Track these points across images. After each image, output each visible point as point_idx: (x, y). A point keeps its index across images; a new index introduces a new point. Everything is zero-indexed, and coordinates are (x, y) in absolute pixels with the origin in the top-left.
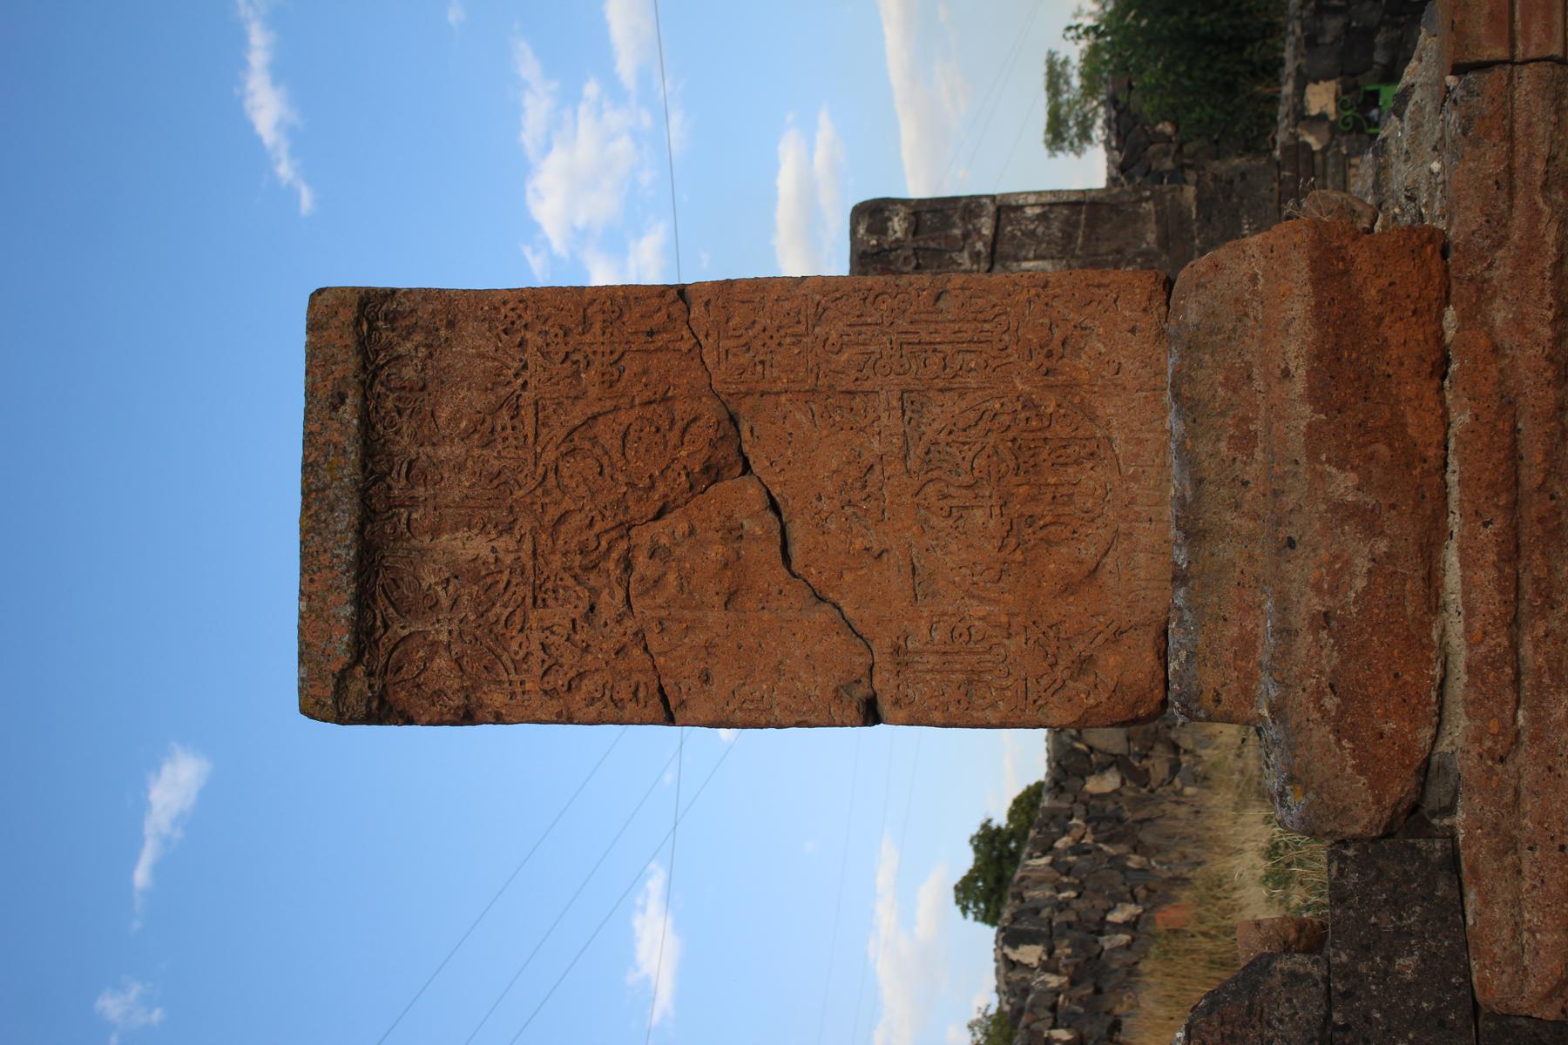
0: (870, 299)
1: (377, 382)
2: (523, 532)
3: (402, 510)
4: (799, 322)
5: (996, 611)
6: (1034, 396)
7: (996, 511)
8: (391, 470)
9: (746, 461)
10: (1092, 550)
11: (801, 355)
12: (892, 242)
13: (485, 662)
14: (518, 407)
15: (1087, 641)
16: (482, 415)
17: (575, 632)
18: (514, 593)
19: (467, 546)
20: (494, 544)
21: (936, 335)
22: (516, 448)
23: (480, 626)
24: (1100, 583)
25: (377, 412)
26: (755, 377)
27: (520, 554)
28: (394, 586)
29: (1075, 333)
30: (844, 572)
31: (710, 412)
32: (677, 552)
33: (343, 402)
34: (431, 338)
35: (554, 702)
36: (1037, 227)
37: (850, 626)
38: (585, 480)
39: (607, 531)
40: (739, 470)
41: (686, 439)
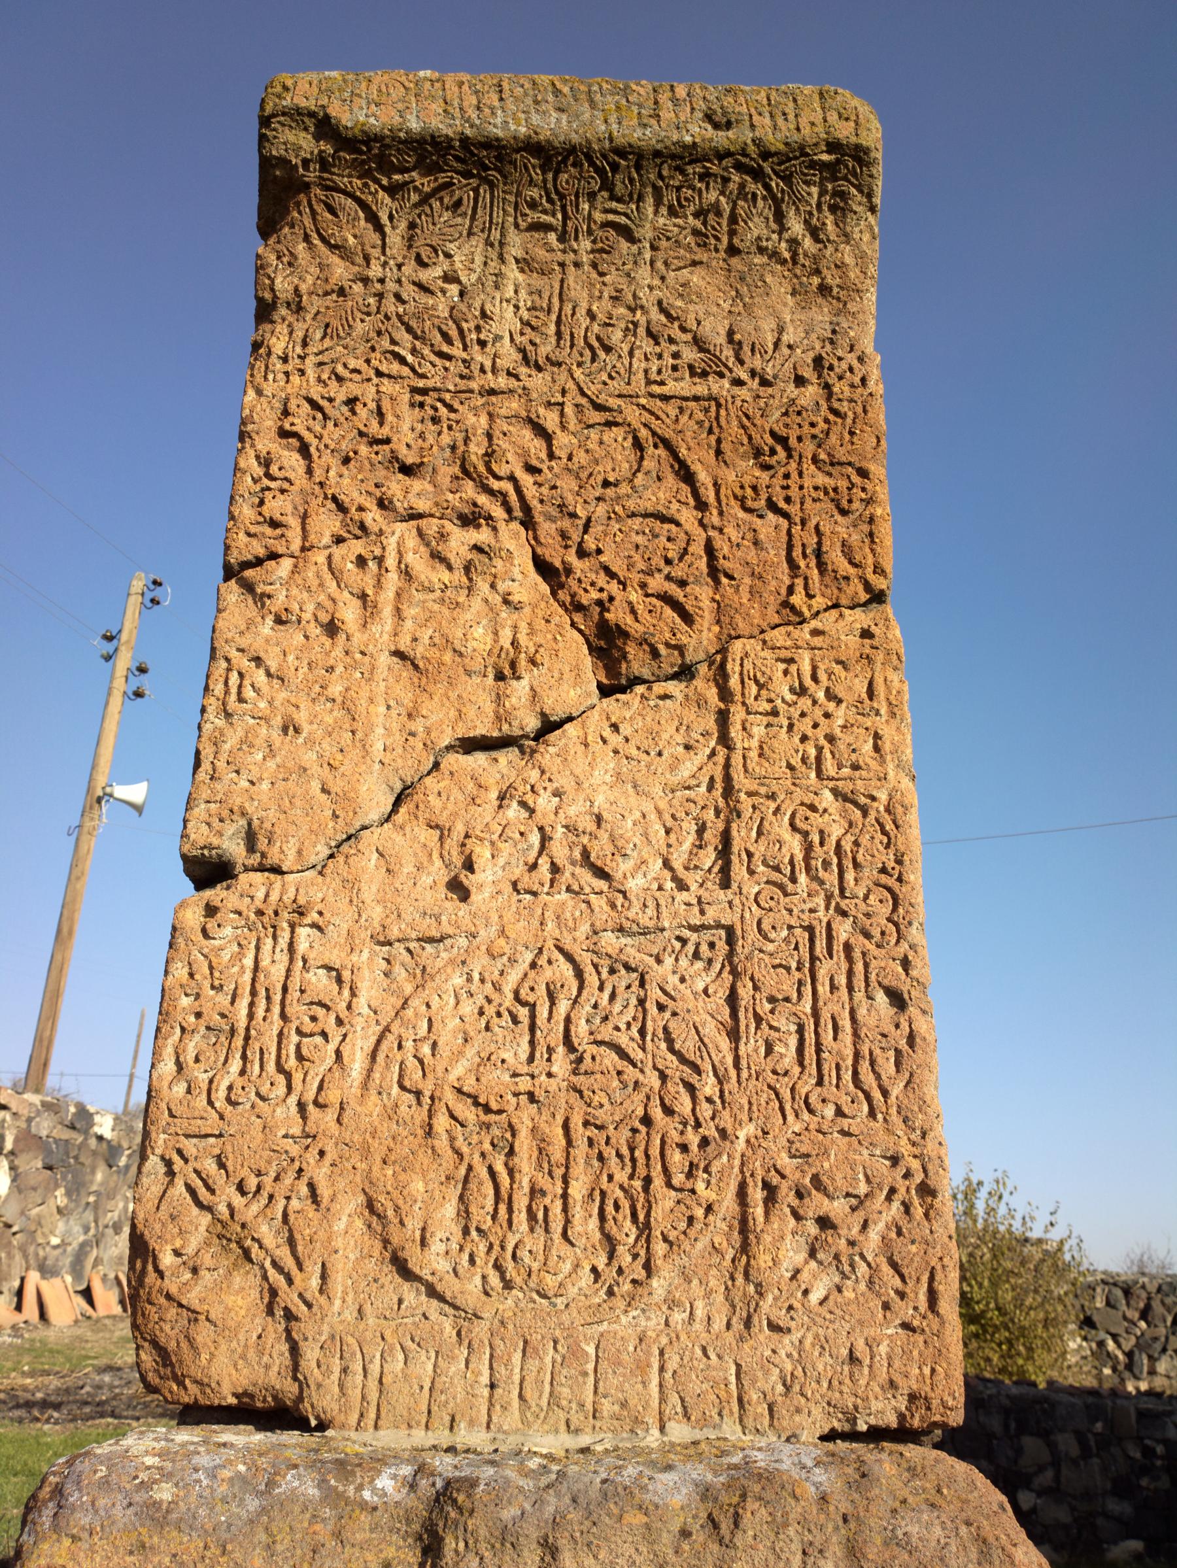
0: (884, 879)
3: (559, 216)
6: (725, 1158)
7: (524, 1084)
8: (619, 200)
21: (828, 988)
26: (750, 701)
29: (843, 1241)
33: (716, 126)
41: (654, 600)
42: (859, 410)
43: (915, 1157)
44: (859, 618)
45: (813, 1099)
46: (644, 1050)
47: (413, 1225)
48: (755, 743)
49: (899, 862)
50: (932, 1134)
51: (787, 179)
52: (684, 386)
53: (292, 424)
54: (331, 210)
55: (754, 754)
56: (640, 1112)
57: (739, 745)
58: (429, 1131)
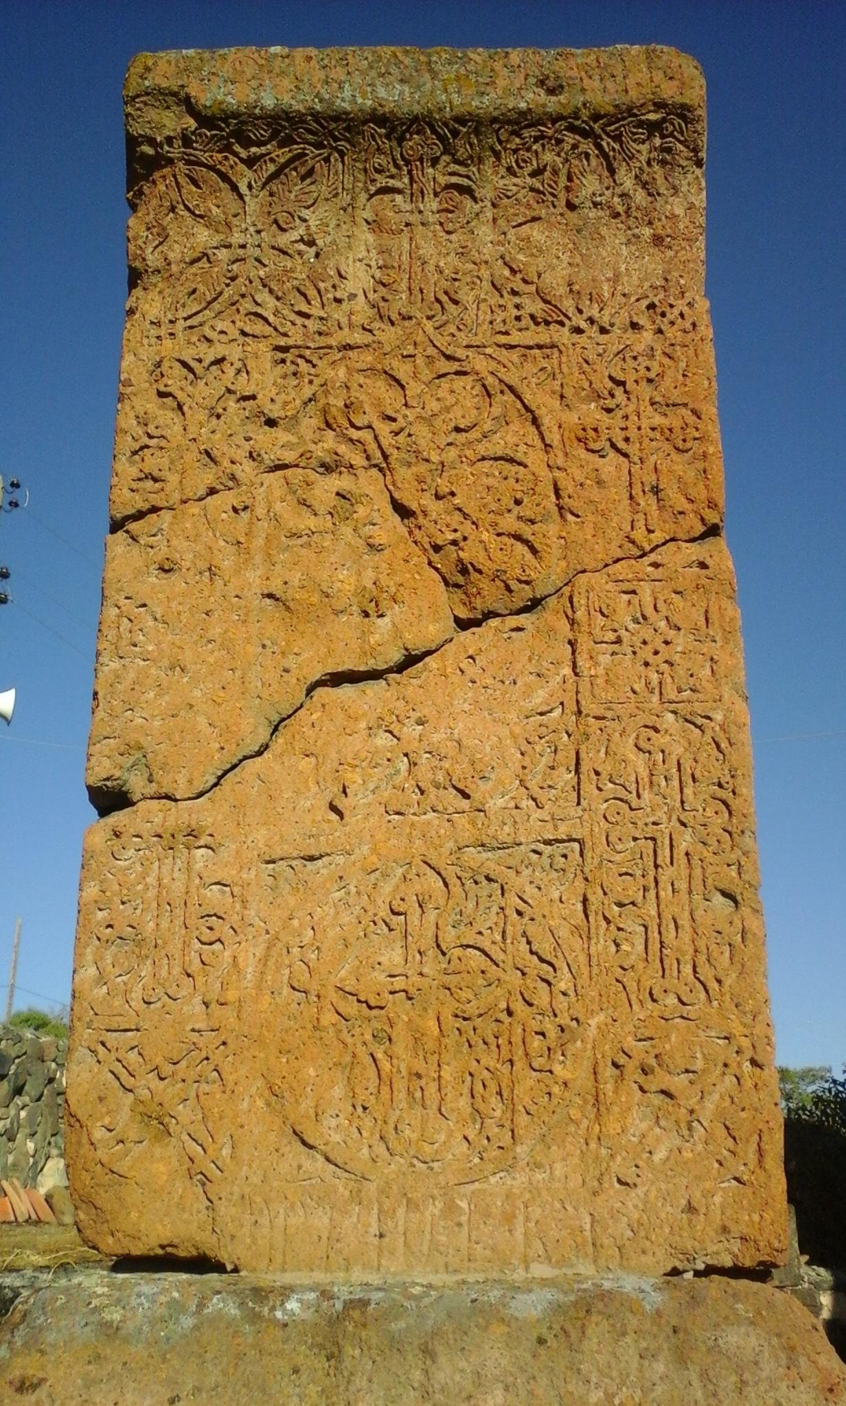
1: (577, 137)
2: (375, 332)
3: (406, 180)
4: (680, 691)
5: (245, 983)
6: (579, 1043)
7: (399, 983)
9: (478, 623)
10: (336, 1138)
11: (631, 694)
13: (201, 288)
14: (547, 323)
15: (191, 1129)
16: (536, 280)
17: (238, 401)
18: (294, 324)
19: (358, 264)
20: (361, 298)
22: (491, 323)
23: (251, 282)
24: (285, 1150)
25: (536, 140)
26: (597, 631)
27: (346, 330)
28: (303, 170)
29: (683, 1110)
30: (313, 760)
31: (548, 575)
32: (346, 530)
33: (551, 92)
34: (639, 216)
35: (145, 376)
37: (234, 767)
38: (447, 410)
39: (376, 437)
40: (464, 614)
41: (505, 539)
42: (691, 352)
44: (695, 551)
47: (306, 1105)
48: (601, 671)
50: (760, 1017)
51: (617, 138)
53: (166, 386)
54: (195, 183)
55: (600, 681)
56: (503, 1005)
57: (585, 673)
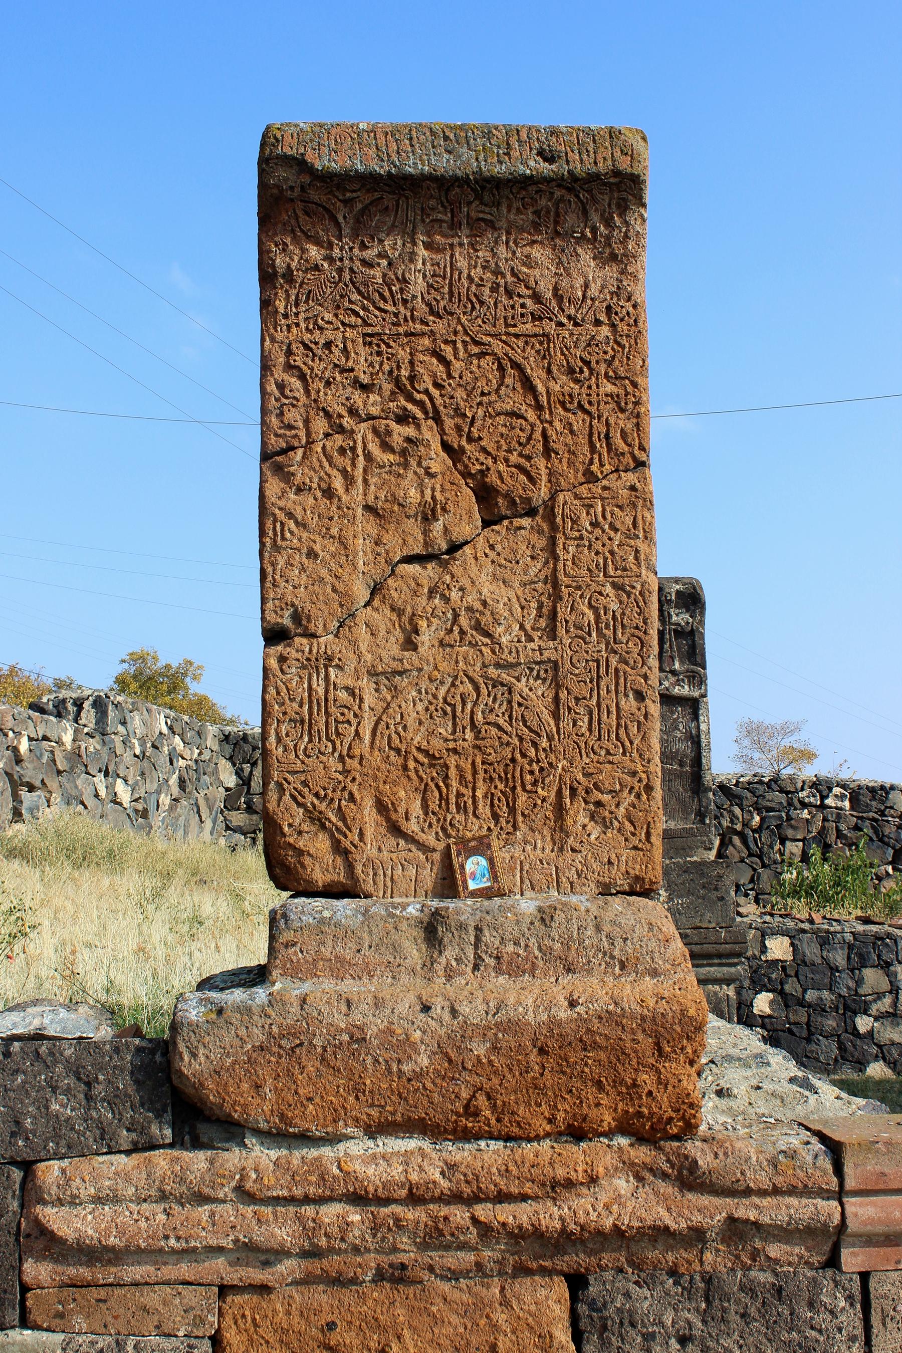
0: (637, 632)
1: (564, 191)
3: (449, 215)
4: (616, 569)
7: (451, 745)
8: (486, 205)
12: (669, 613)
25: (537, 192)
26: (568, 531)
33: (546, 160)
36: (679, 730)
41: (513, 469)
42: (633, 342)
43: (644, 772)
44: (630, 478)
45: (595, 747)
46: (511, 726)
48: (570, 557)
49: (645, 623)
51: (589, 191)
52: (528, 327)
53: (295, 361)
55: (569, 563)
56: (510, 756)
57: (562, 558)
58: (405, 768)
